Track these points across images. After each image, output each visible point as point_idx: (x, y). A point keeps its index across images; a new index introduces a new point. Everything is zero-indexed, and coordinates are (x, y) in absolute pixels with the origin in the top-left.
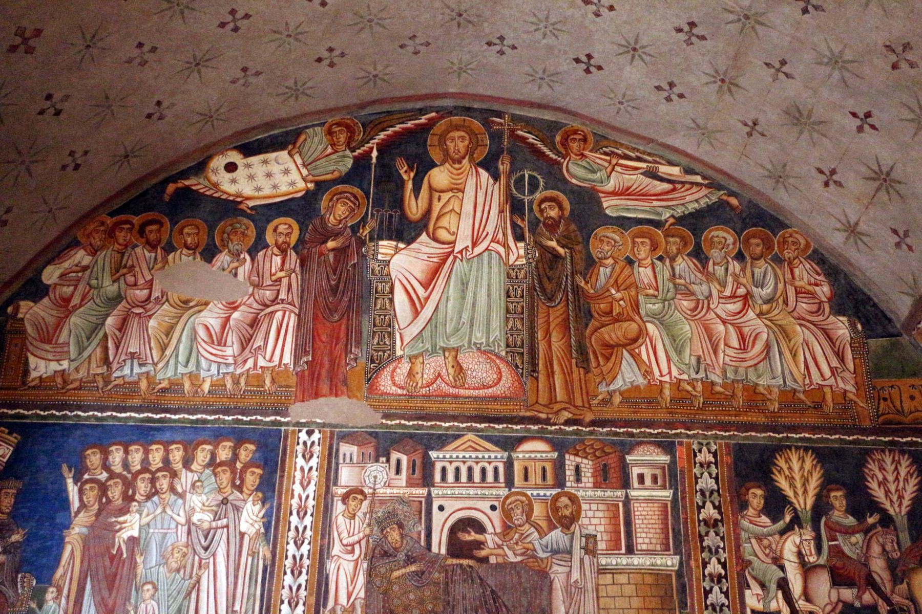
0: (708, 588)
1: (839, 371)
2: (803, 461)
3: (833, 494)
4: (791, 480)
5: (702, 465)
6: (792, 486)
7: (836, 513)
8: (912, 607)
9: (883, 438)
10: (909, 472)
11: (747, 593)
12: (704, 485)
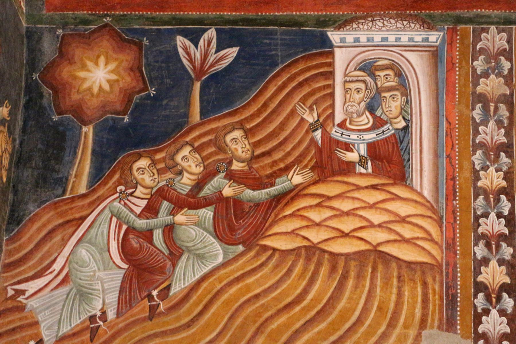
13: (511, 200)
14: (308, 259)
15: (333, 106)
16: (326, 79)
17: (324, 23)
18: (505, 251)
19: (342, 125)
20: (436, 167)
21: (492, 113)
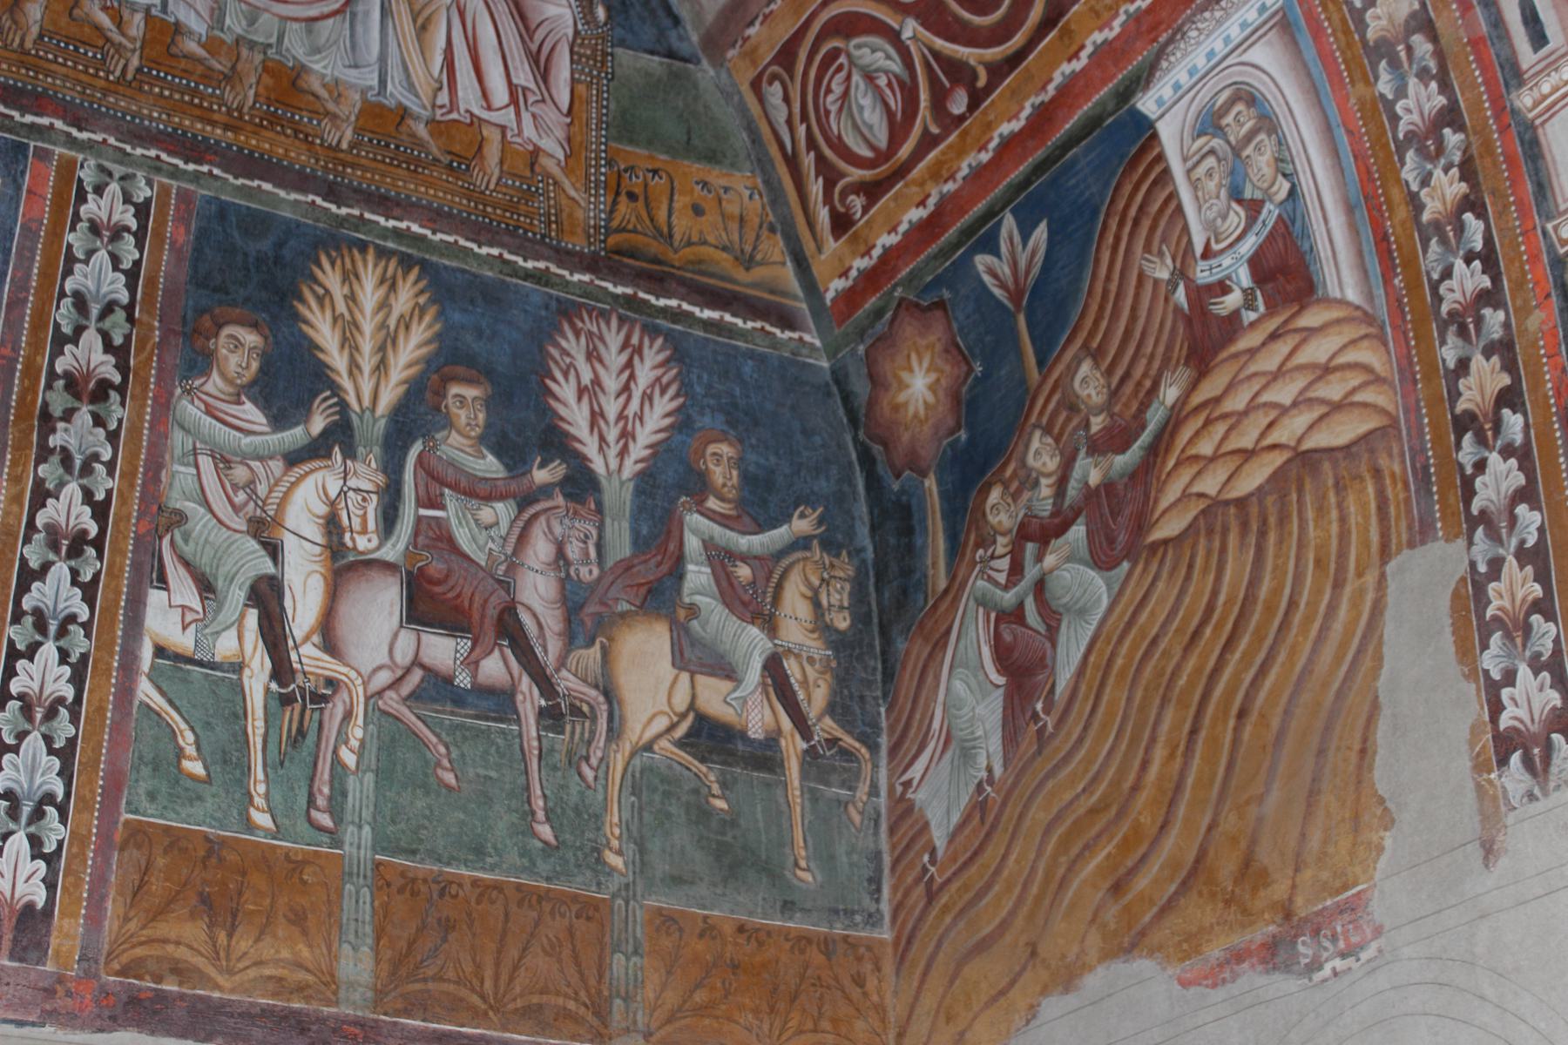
0: (34, 564)
1: (531, 99)
2: (393, 287)
3: (455, 389)
4: (349, 332)
5: (95, 228)
6: (349, 342)
7: (455, 438)
8: (605, 707)
9: (610, 286)
10: (658, 379)
11: (155, 597)
12: (91, 284)
13: (1481, 214)
14: (1210, 532)
15: (1186, 229)
16: (1163, 188)
17: (1126, 94)
19: (1207, 254)
20: (1353, 228)
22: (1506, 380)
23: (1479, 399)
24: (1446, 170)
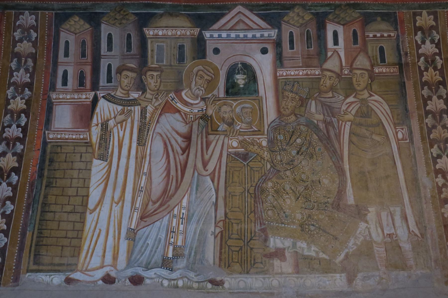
13: (27, 117)
18: (18, 147)
21: (23, 64)
22: (17, 165)
23: (6, 166)
24: (21, 99)
